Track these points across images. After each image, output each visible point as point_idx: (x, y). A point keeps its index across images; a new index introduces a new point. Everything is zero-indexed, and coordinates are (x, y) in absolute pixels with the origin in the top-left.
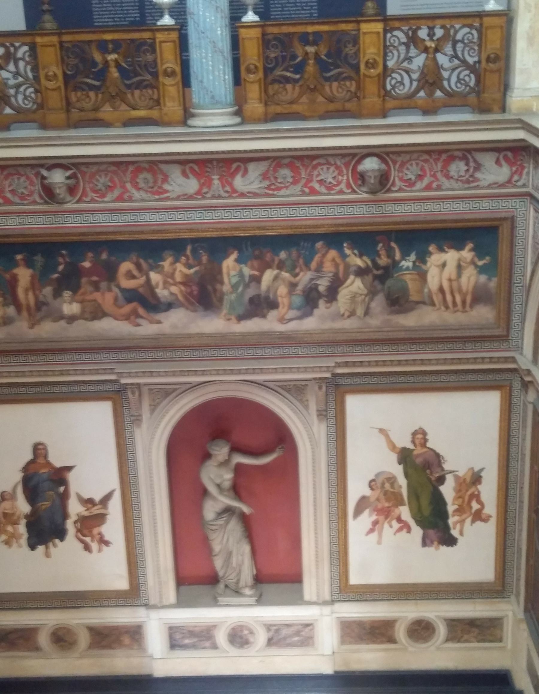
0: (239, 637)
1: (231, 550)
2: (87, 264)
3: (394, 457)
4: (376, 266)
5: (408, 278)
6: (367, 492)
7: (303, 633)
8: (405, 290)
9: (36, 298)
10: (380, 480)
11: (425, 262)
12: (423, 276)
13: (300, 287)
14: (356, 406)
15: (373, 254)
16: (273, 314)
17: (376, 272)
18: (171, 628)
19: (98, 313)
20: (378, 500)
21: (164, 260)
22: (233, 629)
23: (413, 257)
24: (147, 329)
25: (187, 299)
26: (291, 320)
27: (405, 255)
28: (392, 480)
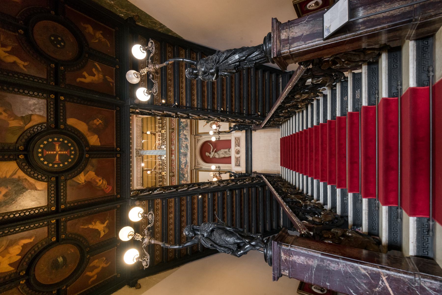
0: (238, 152)
1: (222, 153)
12: (184, 122)
14: (200, 132)
15: (181, 130)
19: (187, 171)
24: (189, 164)
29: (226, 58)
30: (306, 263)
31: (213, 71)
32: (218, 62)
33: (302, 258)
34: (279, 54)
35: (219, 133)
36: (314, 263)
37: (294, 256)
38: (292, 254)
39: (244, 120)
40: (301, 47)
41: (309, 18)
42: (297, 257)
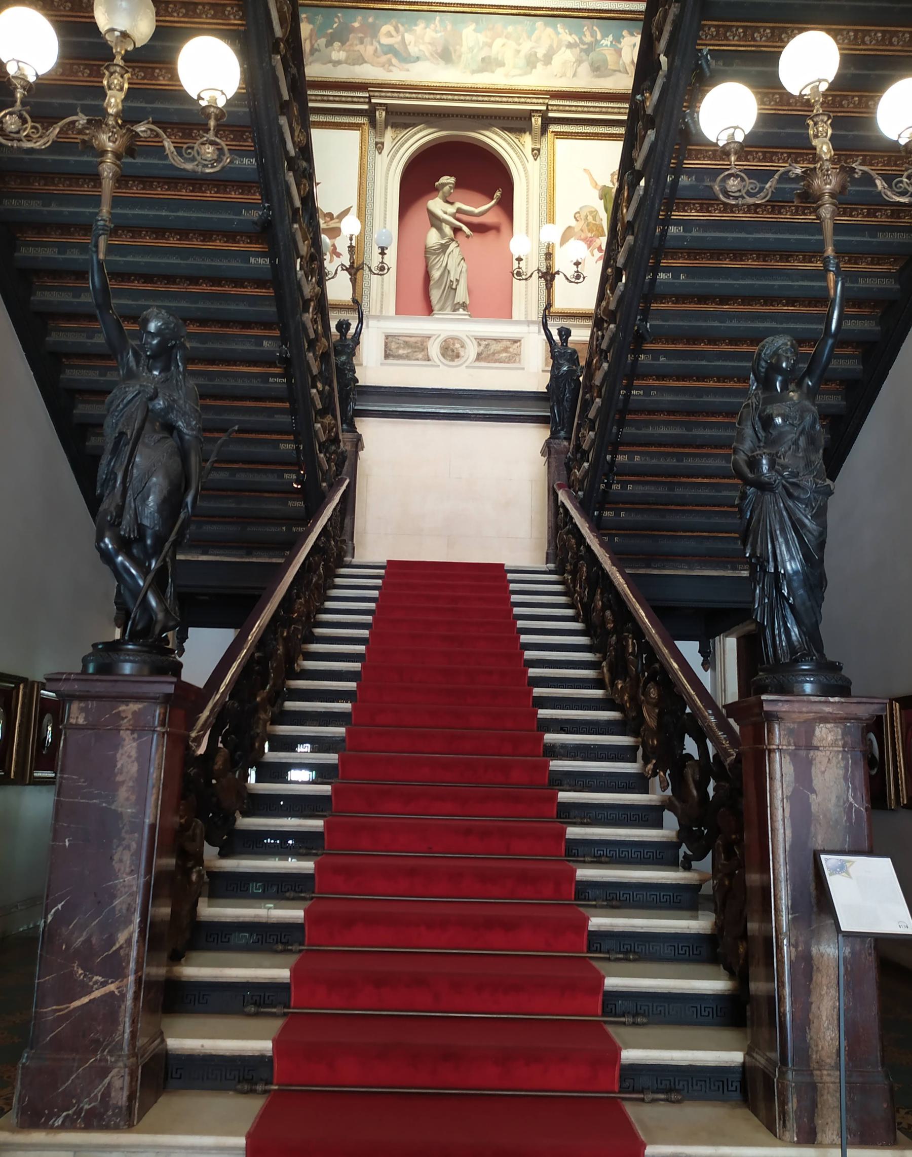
0: (450, 351)
2: (356, 25)
3: (596, 194)
4: (584, 43)
5: (606, 52)
6: (573, 223)
7: (511, 350)
8: (605, 61)
9: (312, 46)
10: (583, 214)
11: (620, 42)
12: (619, 52)
13: (522, 54)
16: (500, 71)
17: (582, 46)
18: (387, 337)
20: (582, 230)
21: (416, 25)
22: (445, 341)
23: (611, 38)
25: (432, 55)
26: (514, 76)
27: (605, 36)
28: (594, 214)
29: (798, 526)
30: (119, 778)
31: (765, 468)
32: (790, 496)
33: (134, 769)
34: (772, 717)
35: (548, 277)
36: (123, 800)
37: (135, 744)
38: (140, 737)
39: (593, 422)
40: (778, 784)
41: (858, 811)
42: (134, 753)
